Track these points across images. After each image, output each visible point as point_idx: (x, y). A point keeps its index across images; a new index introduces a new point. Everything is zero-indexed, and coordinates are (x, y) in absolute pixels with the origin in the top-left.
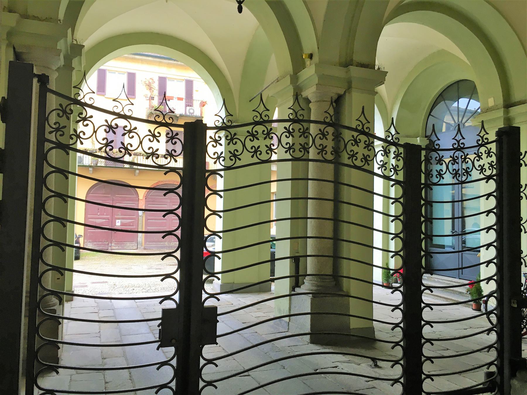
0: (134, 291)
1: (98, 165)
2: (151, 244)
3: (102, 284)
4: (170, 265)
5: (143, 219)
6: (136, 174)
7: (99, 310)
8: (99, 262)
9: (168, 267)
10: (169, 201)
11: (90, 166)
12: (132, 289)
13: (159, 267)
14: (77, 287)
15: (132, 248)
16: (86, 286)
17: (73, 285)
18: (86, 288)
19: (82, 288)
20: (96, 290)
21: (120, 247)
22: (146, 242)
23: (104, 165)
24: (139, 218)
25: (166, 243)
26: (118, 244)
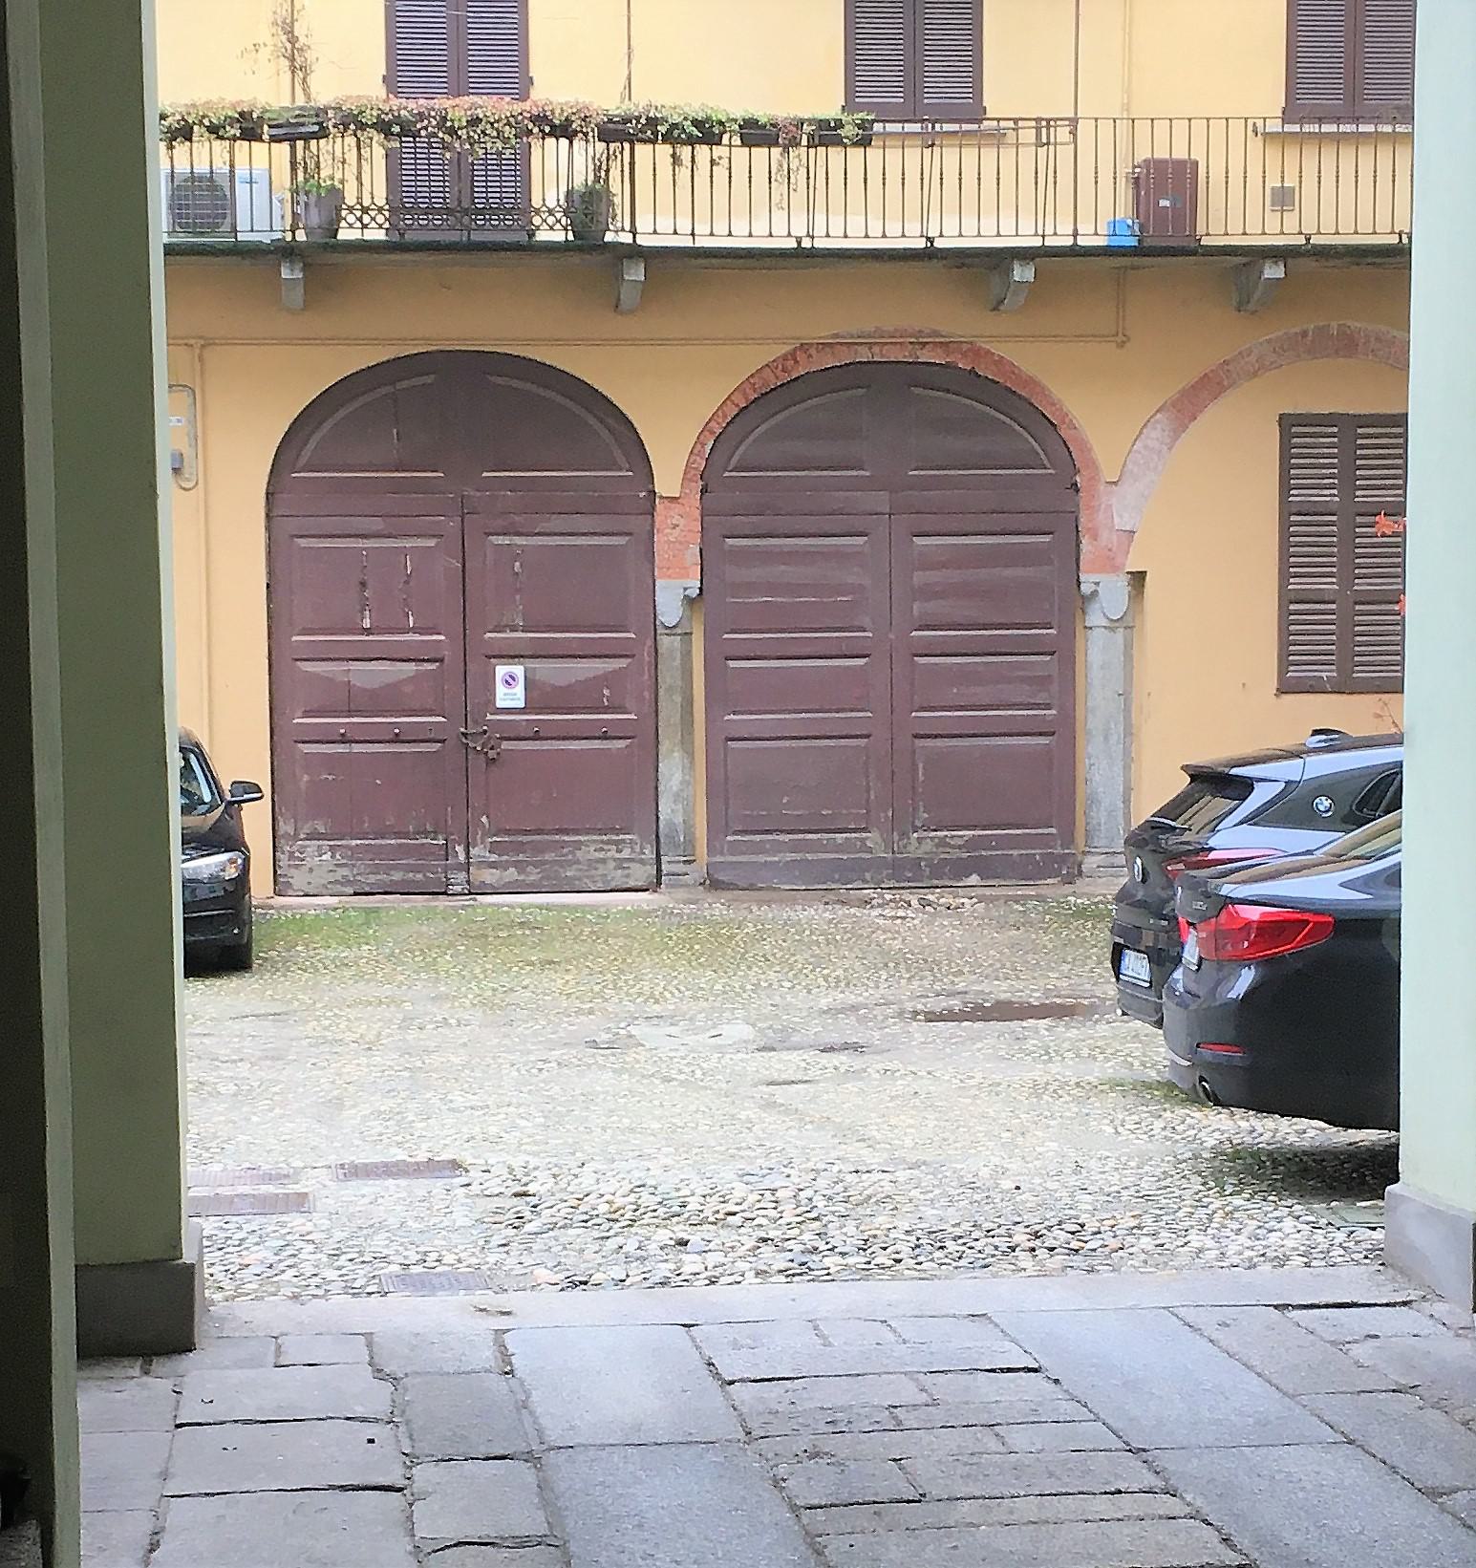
0: (691, 1263)
1: (344, 235)
2: (758, 848)
3: (421, 1186)
4: (932, 1017)
5: (687, 655)
6: (628, 296)
7: (411, 1459)
8: (388, 990)
9: (919, 1029)
10: (881, 500)
11: (286, 251)
12: (663, 1236)
13: (848, 1030)
14: (221, 1206)
15: (618, 878)
16: (299, 1203)
17: (187, 1195)
18: (296, 1221)
19: (270, 1223)
20: (379, 1243)
21: (533, 876)
22: (715, 830)
23: (380, 235)
24: (665, 642)
25: (873, 838)
26: (520, 848)
